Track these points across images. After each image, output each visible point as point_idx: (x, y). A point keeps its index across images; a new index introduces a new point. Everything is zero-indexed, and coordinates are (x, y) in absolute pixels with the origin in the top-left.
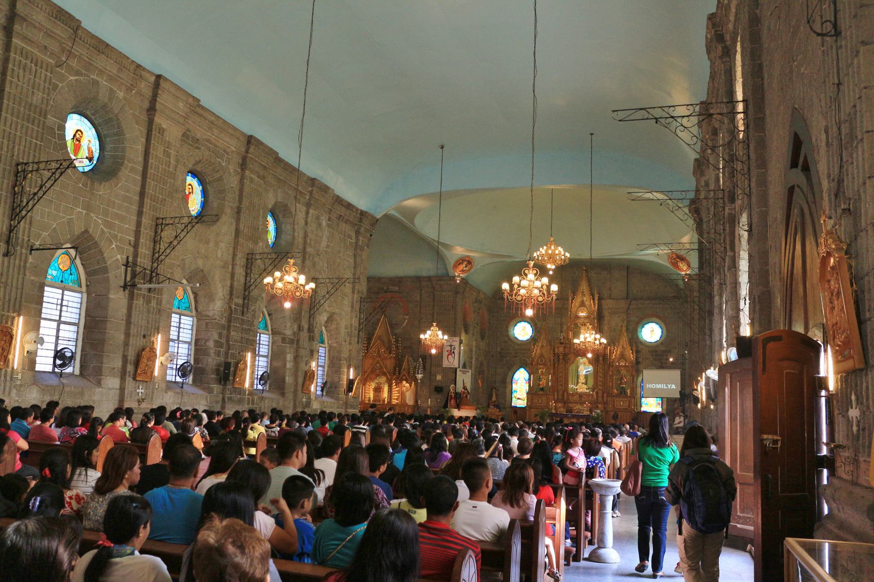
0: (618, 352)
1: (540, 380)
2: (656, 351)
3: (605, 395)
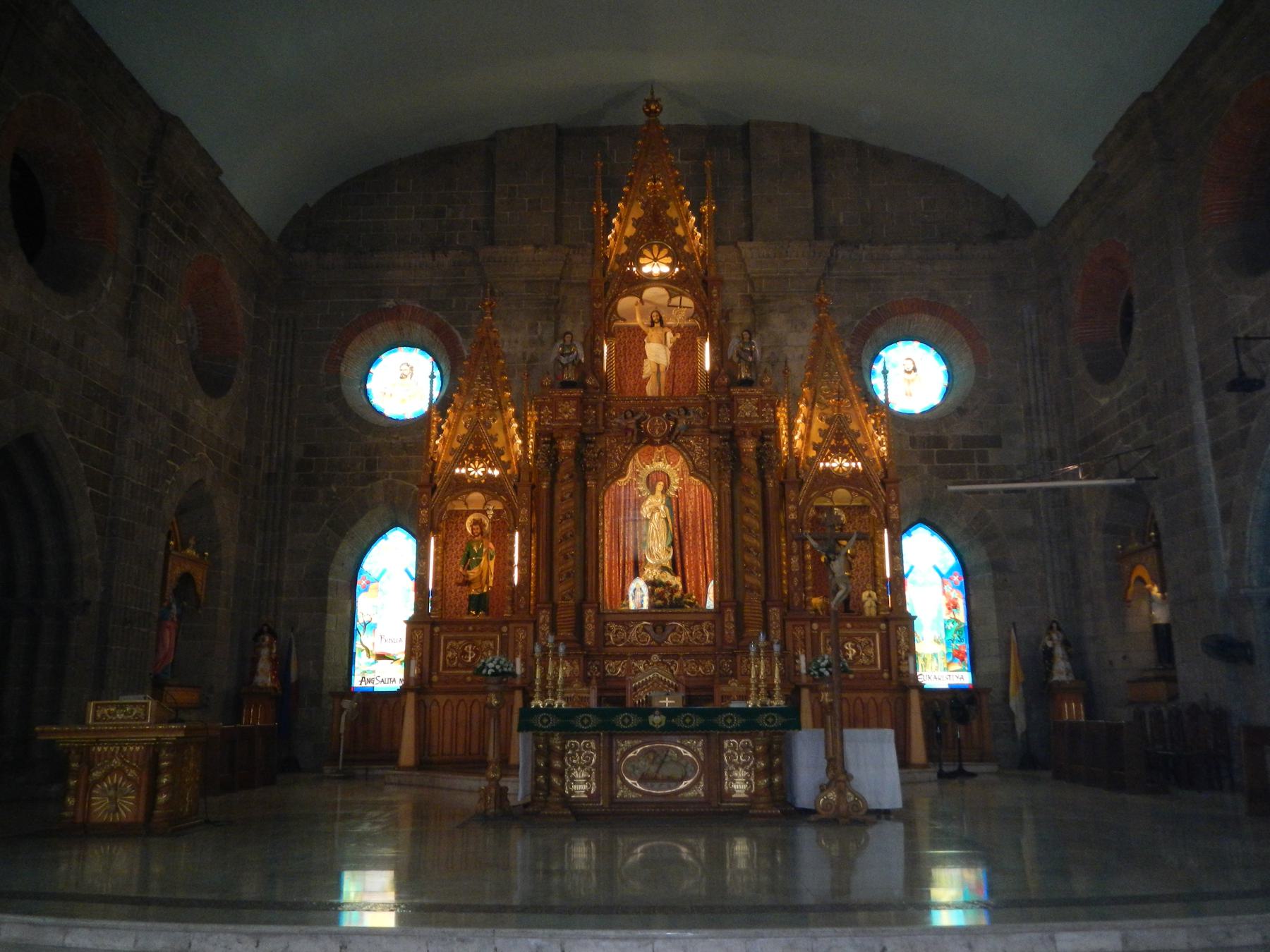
0: (818, 424)
1: (469, 558)
2: (939, 442)
3: (775, 614)
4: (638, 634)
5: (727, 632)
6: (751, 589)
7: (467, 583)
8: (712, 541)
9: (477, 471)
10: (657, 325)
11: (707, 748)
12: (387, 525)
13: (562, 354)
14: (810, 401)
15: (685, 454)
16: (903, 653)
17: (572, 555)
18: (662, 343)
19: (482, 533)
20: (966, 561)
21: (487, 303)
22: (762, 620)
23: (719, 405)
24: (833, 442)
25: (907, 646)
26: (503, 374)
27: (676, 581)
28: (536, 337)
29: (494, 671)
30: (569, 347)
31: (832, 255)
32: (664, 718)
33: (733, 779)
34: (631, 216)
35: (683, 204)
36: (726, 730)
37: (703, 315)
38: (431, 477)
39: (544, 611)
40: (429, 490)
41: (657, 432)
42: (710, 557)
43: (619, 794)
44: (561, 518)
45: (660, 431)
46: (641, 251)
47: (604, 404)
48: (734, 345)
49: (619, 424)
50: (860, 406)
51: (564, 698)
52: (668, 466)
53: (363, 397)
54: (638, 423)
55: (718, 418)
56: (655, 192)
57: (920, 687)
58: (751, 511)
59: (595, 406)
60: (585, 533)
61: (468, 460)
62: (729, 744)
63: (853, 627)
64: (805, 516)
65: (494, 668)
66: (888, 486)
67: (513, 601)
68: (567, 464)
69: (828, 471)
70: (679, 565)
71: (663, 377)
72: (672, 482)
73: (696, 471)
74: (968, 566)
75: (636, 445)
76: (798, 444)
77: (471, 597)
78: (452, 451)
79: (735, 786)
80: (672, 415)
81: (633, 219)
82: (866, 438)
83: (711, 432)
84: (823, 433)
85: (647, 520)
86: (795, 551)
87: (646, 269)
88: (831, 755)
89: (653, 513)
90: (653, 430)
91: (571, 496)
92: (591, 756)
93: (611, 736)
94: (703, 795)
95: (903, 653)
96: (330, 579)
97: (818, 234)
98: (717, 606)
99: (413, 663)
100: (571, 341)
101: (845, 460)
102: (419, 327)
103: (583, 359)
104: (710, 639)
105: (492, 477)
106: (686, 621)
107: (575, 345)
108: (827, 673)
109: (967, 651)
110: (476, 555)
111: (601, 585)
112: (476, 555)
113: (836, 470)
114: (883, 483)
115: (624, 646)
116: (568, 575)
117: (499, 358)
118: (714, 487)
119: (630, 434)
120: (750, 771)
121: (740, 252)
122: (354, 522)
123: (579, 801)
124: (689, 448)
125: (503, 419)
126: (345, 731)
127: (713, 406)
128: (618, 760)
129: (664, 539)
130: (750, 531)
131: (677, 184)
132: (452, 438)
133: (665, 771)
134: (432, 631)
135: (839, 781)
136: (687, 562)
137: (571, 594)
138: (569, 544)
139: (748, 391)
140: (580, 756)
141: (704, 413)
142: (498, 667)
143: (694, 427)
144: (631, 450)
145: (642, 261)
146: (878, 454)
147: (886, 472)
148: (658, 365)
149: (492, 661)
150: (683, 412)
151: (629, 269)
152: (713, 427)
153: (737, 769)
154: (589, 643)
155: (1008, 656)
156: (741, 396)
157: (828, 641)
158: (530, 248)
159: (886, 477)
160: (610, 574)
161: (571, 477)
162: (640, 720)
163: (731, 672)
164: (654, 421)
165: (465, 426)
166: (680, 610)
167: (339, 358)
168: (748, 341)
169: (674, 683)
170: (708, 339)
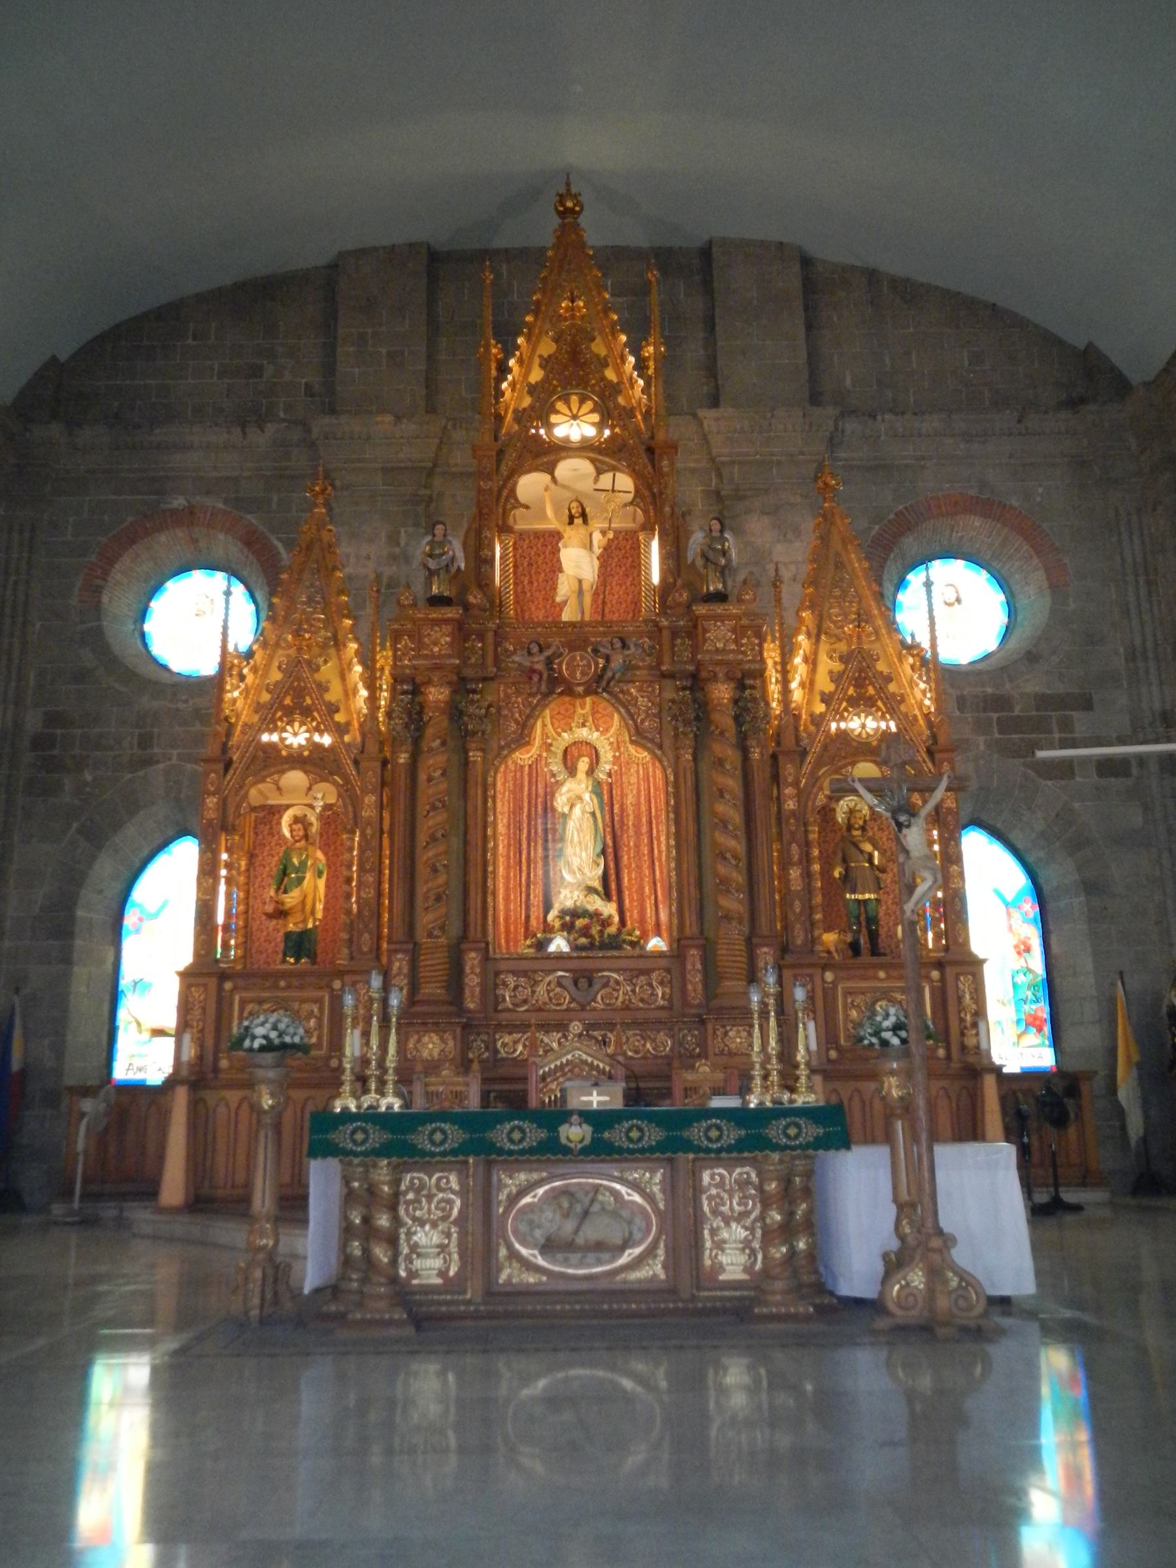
0: (827, 665)
1: (285, 877)
2: (1000, 702)
3: (766, 955)
4: (549, 992)
5: (690, 987)
6: (727, 917)
7: (281, 913)
8: (663, 848)
9: (296, 737)
10: (578, 521)
11: (671, 1187)
12: (171, 833)
13: (431, 556)
14: (814, 632)
15: (622, 710)
16: (968, 1018)
17: (445, 866)
18: (585, 548)
19: (306, 837)
20: (1041, 881)
21: (317, 488)
22: (744, 966)
23: (675, 634)
24: (851, 691)
25: (974, 1006)
26: (341, 592)
27: (609, 909)
28: (397, 550)
29: (264, 1042)
30: (441, 544)
31: (836, 429)
32: (587, 1130)
33: (720, 1245)
34: (538, 352)
35: (615, 338)
36: (708, 1150)
37: (649, 500)
38: (225, 748)
39: (400, 956)
40: (221, 766)
41: (578, 675)
42: (661, 873)
43: (503, 1277)
44: (428, 807)
45: (583, 674)
46: (553, 405)
47: (495, 632)
48: (697, 540)
49: (520, 664)
50: (891, 638)
51: (398, 1094)
52: (596, 734)
53: (139, 642)
54: (549, 662)
55: (673, 653)
56: (573, 317)
57: (997, 1070)
58: (727, 797)
59: (481, 637)
60: (466, 833)
61: (282, 721)
62: (712, 1177)
63: (888, 977)
64: (810, 804)
65: (265, 1037)
66: (938, 756)
67: (351, 941)
68: (437, 725)
69: (843, 735)
70: (613, 886)
71: (588, 599)
72: (603, 759)
73: (639, 736)
74: (1046, 889)
75: (546, 696)
76: (797, 695)
77: (288, 936)
78: (258, 707)
79: (724, 1259)
80: (602, 650)
81: (540, 356)
82: (901, 686)
83: (664, 676)
84: (836, 678)
85: (565, 816)
86: (796, 858)
87: (560, 432)
88: (904, 1196)
89: (572, 807)
90: (573, 675)
91: (443, 774)
92: (450, 1202)
93: (489, 1164)
94: (663, 1276)
95: (968, 1018)
96: (80, 913)
97: (815, 398)
98: (675, 946)
99: (187, 1038)
100: (445, 535)
101: (870, 718)
102: (221, 537)
103: (463, 566)
104: (663, 998)
105: (318, 747)
106: (624, 970)
107: (450, 542)
108: (895, 1041)
109: (1045, 1014)
110: (297, 870)
111: (490, 913)
112: (297, 870)
113: (856, 733)
114: (930, 752)
115: (527, 1011)
116: (438, 898)
117: (335, 568)
118: (668, 760)
119: (536, 678)
120: (751, 1229)
121: (701, 424)
122: (117, 826)
123: (428, 1290)
124: (629, 702)
125: (340, 659)
126: (86, 1152)
127: (666, 634)
128: (501, 1210)
129: (591, 845)
130: (726, 827)
131: (606, 311)
132: (258, 690)
133: (591, 1232)
134: (220, 989)
135: (933, 1250)
136: (626, 880)
137: (442, 928)
138: (442, 848)
139: (719, 609)
140: (429, 1202)
141: (653, 647)
142: (273, 1035)
143: (638, 668)
144: (537, 705)
145: (554, 419)
146: (921, 709)
147: (934, 736)
148: (580, 581)
149: (263, 1024)
150: (618, 645)
151: (533, 431)
152: (664, 668)
153: (727, 1224)
154: (472, 1006)
155: (1113, 1021)
156: (707, 617)
157: (849, 1000)
158: (389, 418)
159: (935, 742)
160: (507, 899)
161: (444, 743)
162: (543, 1134)
163: (698, 1050)
164: (574, 658)
165: (279, 667)
166: (615, 953)
167: (99, 582)
168: (718, 534)
169: (607, 1069)
170: (657, 537)
